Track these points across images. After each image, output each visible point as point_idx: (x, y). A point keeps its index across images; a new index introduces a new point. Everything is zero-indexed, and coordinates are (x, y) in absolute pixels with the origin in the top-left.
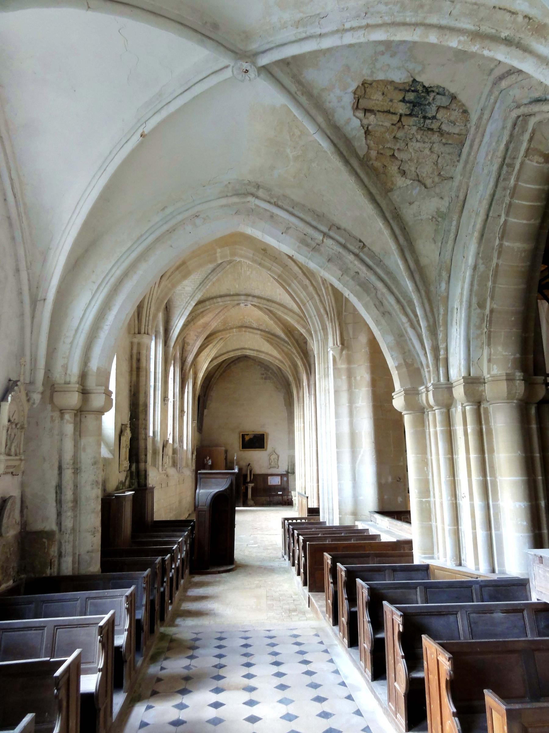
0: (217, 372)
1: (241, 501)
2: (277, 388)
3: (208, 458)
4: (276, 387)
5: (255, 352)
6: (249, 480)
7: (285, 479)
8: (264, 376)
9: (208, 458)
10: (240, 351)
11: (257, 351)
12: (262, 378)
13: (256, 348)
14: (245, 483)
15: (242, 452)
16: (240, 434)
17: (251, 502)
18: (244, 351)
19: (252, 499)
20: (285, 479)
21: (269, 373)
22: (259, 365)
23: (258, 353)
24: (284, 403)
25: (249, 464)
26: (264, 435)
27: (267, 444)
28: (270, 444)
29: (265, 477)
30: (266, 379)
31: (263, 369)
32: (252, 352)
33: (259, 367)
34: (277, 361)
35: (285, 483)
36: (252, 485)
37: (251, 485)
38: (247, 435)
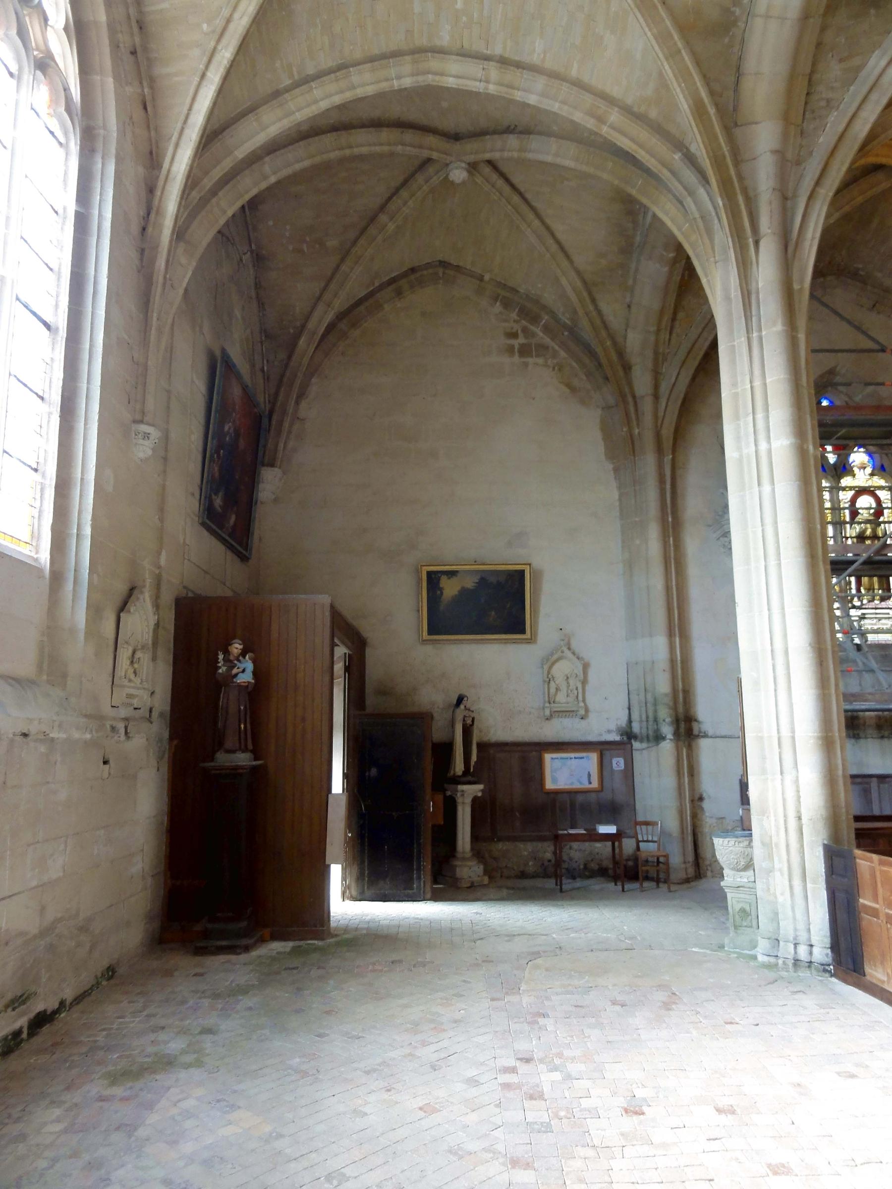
0: (320, 308)
1: (427, 865)
2: (573, 389)
3: (236, 647)
4: (569, 386)
5: (494, 72)
6: (459, 767)
7: (618, 763)
8: (516, 343)
9: (236, 647)
10: (406, 66)
11: (503, 62)
12: (510, 350)
13: (497, 50)
14: (444, 780)
15: (429, 649)
16: (418, 571)
17: (469, 870)
18: (434, 63)
19: (478, 854)
20: (618, 763)
21: (538, 331)
22: (496, 298)
23: (512, 75)
24: (602, 449)
26: (522, 572)
28: (549, 612)
29: (531, 753)
30: (524, 351)
31: (514, 315)
32: (474, 68)
33: (498, 307)
34: (615, 116)
36: (475, 790)
37: (470, 791)
38: (452, 574)
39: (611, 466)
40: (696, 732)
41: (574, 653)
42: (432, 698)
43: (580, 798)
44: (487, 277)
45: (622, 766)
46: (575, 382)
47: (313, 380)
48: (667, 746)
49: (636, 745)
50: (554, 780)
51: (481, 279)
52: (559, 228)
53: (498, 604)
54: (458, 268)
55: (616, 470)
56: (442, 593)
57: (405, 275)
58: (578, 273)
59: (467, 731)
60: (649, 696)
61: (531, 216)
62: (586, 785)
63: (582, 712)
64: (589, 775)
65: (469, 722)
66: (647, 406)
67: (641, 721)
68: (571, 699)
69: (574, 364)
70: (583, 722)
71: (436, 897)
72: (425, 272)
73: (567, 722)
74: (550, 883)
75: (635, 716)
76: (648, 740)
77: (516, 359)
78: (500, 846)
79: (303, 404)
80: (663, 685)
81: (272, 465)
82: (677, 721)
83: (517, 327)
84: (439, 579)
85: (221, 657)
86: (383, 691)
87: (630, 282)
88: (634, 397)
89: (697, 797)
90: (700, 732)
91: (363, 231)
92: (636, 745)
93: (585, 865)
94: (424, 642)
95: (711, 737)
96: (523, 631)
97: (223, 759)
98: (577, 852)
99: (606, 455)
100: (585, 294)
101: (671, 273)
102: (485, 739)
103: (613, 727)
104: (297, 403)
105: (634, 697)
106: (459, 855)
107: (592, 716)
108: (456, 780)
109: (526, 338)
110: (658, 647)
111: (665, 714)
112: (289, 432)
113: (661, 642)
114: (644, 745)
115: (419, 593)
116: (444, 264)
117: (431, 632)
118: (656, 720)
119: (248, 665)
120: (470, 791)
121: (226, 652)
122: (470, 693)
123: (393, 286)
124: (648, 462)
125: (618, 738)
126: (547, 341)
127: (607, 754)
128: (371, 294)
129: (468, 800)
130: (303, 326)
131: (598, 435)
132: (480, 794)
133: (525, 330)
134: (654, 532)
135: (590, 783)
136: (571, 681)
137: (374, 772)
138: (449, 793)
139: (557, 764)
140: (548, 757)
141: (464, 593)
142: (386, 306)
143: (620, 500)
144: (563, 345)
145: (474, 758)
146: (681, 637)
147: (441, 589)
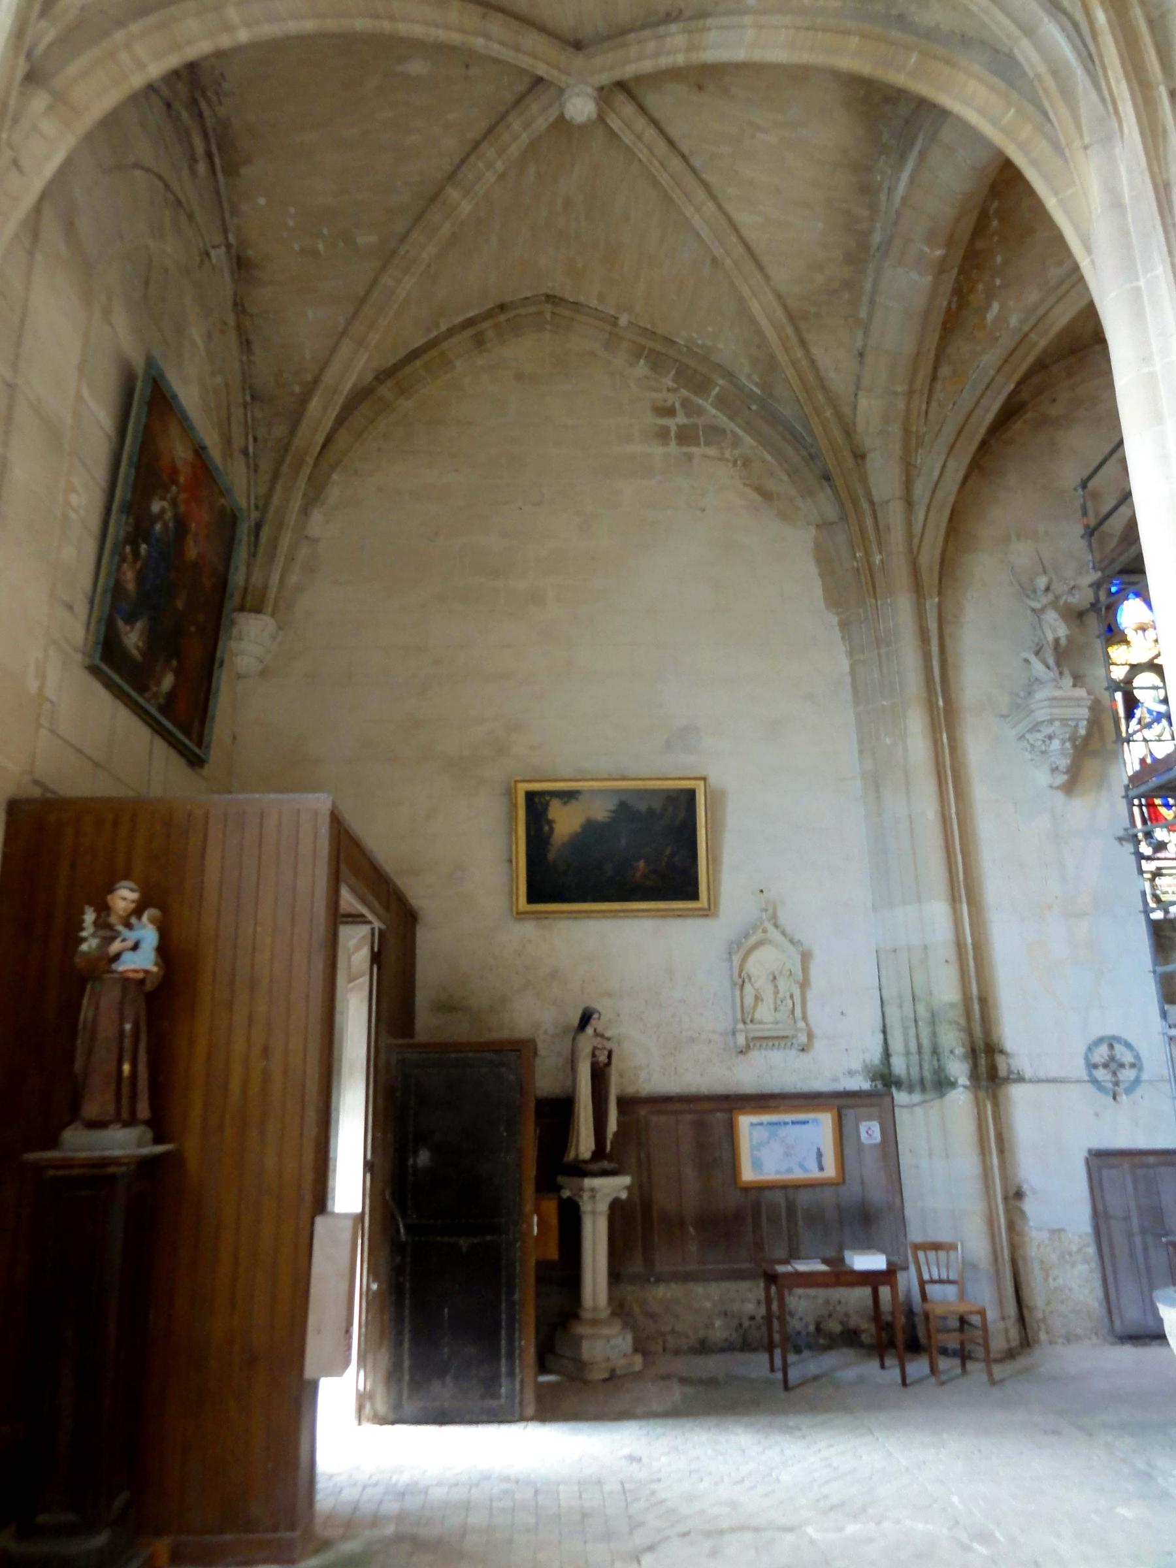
1: (528, 1345)
2: (766, 495)
6: (584, 1144)
7: (870, 1132)
8: (671, 423)
9: (124, 897)
12: (663, 435)
14: (557, 1168)
15: (529, 928)
16: (510, 793)
17: (606, 1345)
20: (870, 1132)
22: (638, 352)
25: (586, 1018)
26: (691, 794)
27: (715, 860)
30: (685, 437)
31: (668, 381)
33: (642, 368)
35: (871, 1169)
37: (608, 1188)
38: (568, 796)
39: (834, 620)
40: (1002, 1072)
41: (784, 933)
42: (535, 1015)
43: (804, 1198)
44: (623, 320)
45: (877, 1137)
46: (770, 484)
47: (335, 477)
48: (960, 1099)
49: (900, 1097)
50: (757, 1164)
51: (614, 321)
52: (744, 218)
53: (642, 853)
54: (576, 306)
55: (844, 625)
56: (552, 830)
57: (488, 315)
58: (779, 297)
59: (599, 1075)
60: (922, 1010)
61: (700, 195)
62: (815, 1174)
63: (803, 1039)
64: (820, 1155)
65: (603, 1058)
66: (895, 515)
67: (908, 1053)
68: (783, 1015)
69: (768, 457)
70: (803, 1056)
71: (549, 1410)
72: (522, 311)
73: (776, 1057)
74: (757, 1365)
75: (896, 1045)
76: (924, 1089)
77: (673, 448)
78: (661, 1291)
79: (317, 516)
80: (946, 989)
81: (258, 610)
82: (973, 1053)
83: (673, 400)
84: (546, 805)
85: (89, 917)
86: (447, 1007)
87: (863, 314)
88: (872, 503)
89: (1011, 1193)
90: (1010, 1072)
91: (418, 218)
92: (900, 1097)
93: (818, 1329)
94: (521, 916)
95: (1031, 1081)
96: (695, 896)
97: (80, 1143)
98: (804, 1305)
99: (826, 599)
100: (790, 330)
101: (936, 284)
102: (630, 1090)
103: (857, 1065)
104: (305, 511)
105: (893, 1014)
106: (587, 1315)
107: (818, 1044)
108: (580, 1170)
109: (688, 415)
110: (935, 919)
111: (952, 1040)
112: (291, 559)
113: (938, 911)
114: (917, 1097)
115: (512, 831)
116: (551, 299)
117: (533, 898)
118: (935, 1051)
119: (148, 935)
120: (608, 1188)
121: (103, 909)
122: (603, 1006)
123: (469, 332)
124: (901, 610)
125: (866, 1086)
126: (722, 420)
127: (850, 1114)
128: (433, 344)
129: (603, 1207)
130: (316, 381)
131: (813, 570)
132: (624, 1195)
133: (685, 403)
134: (916, 723)
135: (821, 1168)
136: (782, 984)
137: (424, 1157)
138: (566, 1194)
139: (761, 1134)
140: (745, 1122)
141: (591, 828)
142: (458, 363)
143: (853, 673)
144: (749, 427)
145: (612, 1125)
146: (969, 903)
147: (550, 823)
